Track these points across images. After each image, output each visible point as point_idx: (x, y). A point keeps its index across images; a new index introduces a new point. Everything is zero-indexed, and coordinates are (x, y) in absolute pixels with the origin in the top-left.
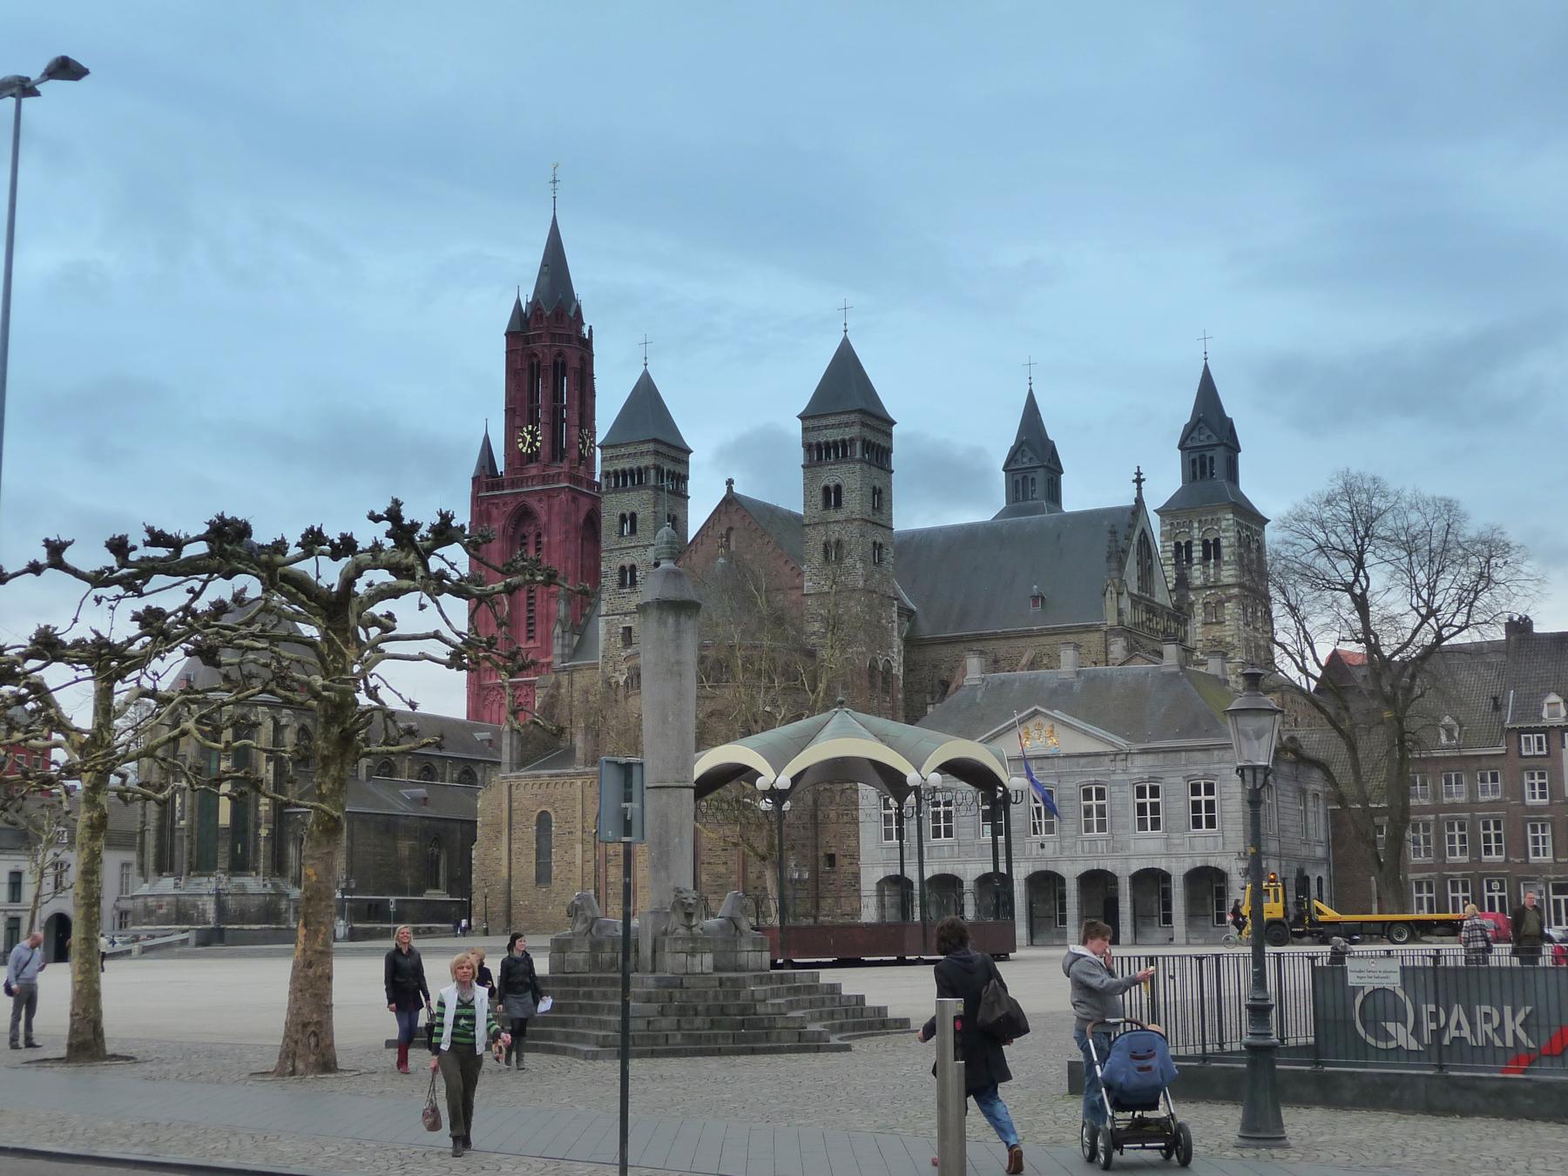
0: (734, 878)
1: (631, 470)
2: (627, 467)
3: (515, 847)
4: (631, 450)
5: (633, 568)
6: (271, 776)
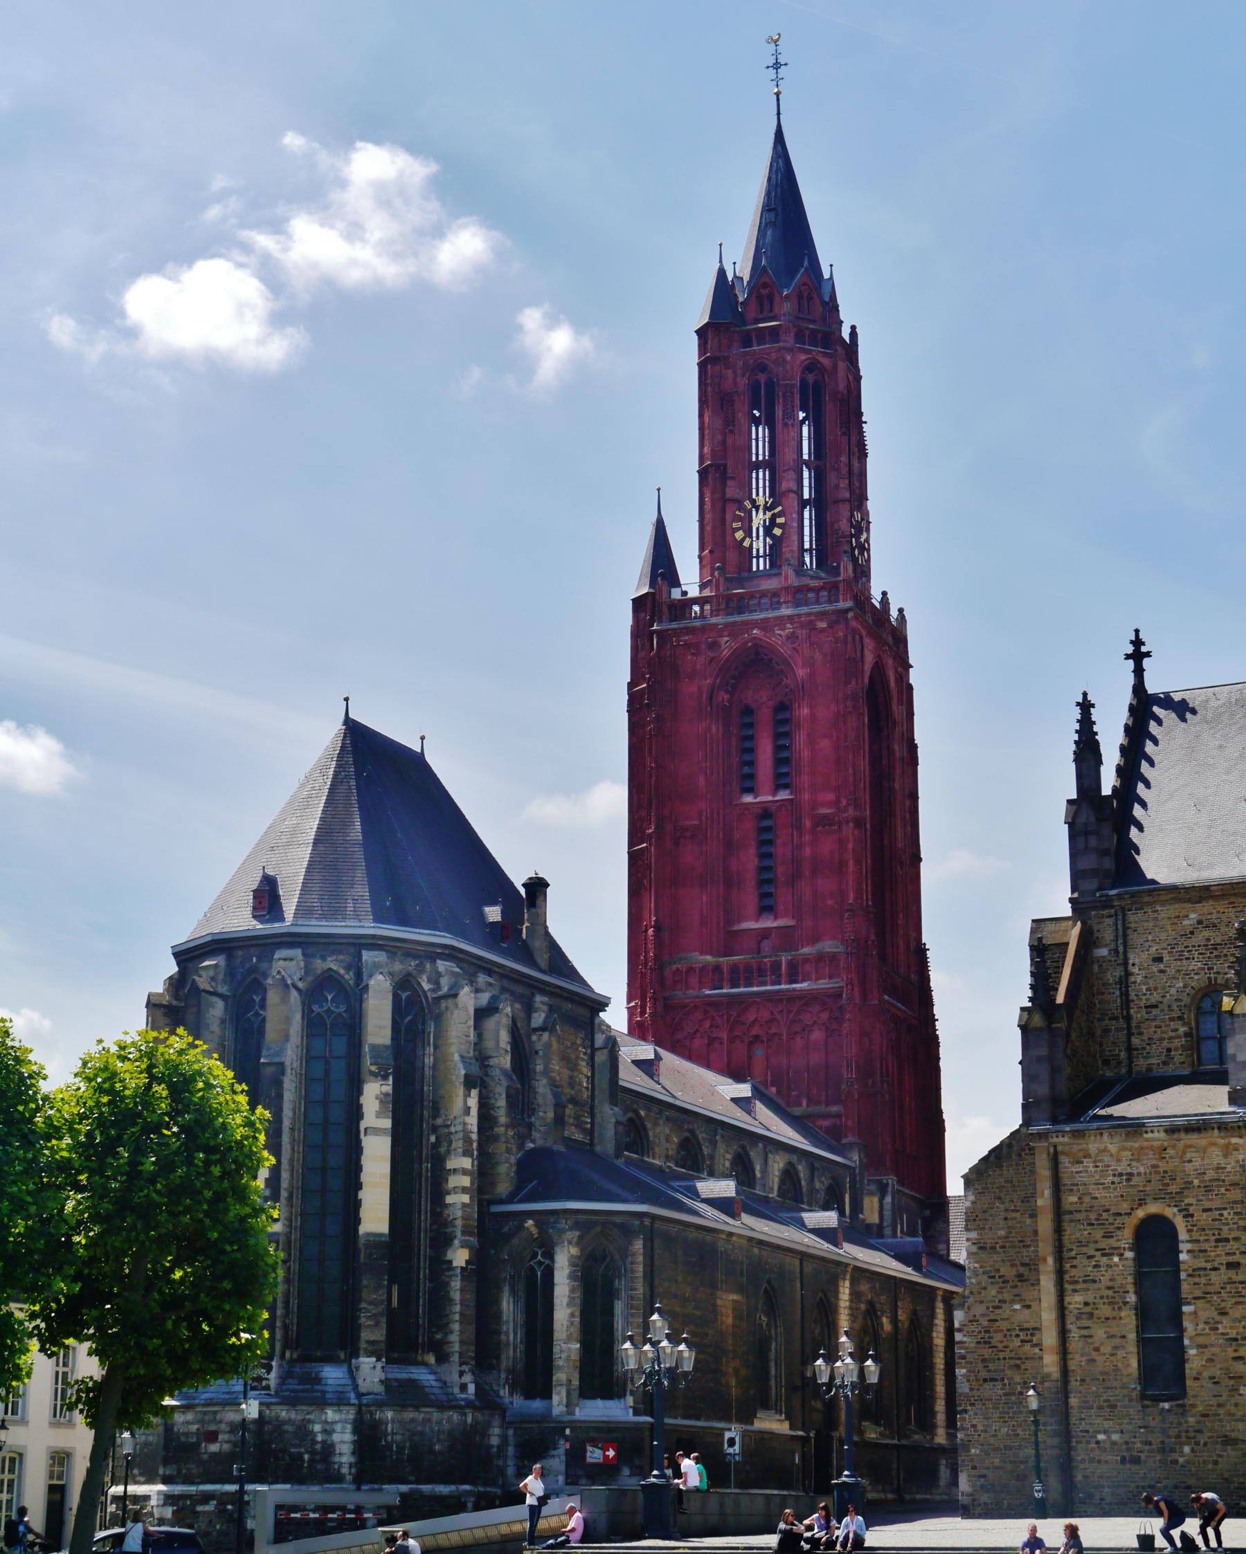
3: (1075, 1301)
6: (473, 1121)
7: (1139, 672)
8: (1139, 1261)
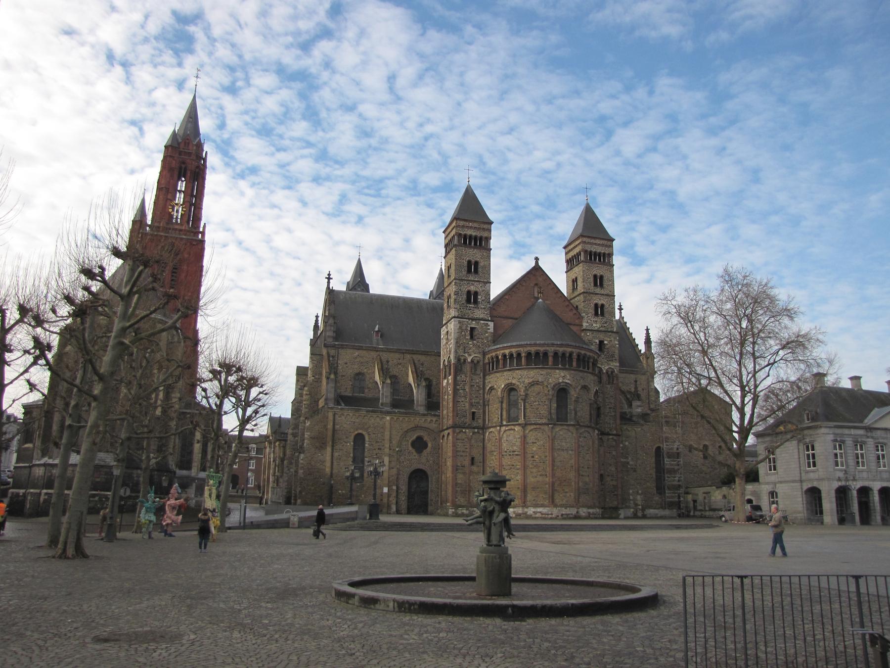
0: (591, 485)
1: (476, 238)
2: (474, 234)
3: (336, 454)
4: (476, 225)
5: (476, 294)
7: (329, 283)
8: (354, 445)
